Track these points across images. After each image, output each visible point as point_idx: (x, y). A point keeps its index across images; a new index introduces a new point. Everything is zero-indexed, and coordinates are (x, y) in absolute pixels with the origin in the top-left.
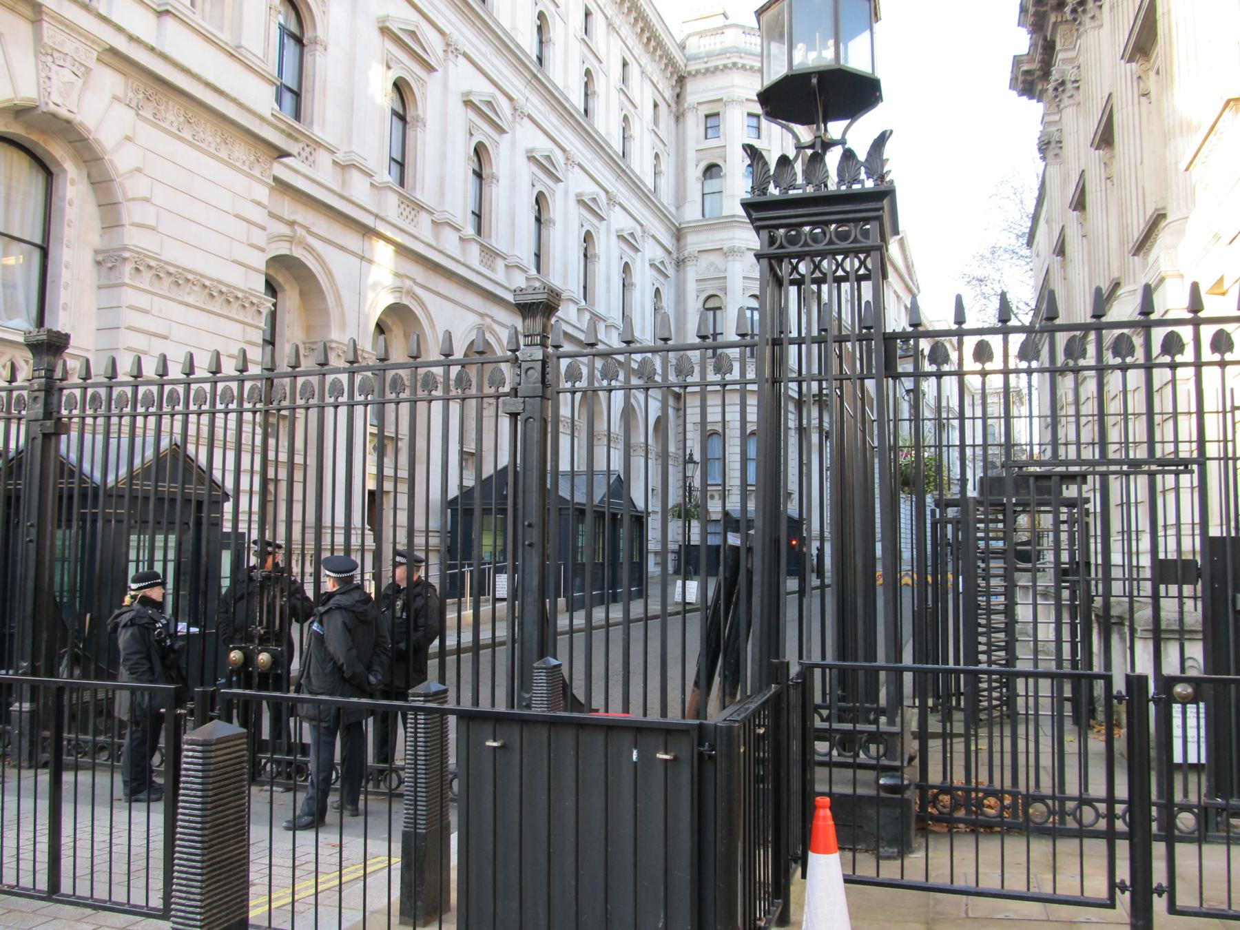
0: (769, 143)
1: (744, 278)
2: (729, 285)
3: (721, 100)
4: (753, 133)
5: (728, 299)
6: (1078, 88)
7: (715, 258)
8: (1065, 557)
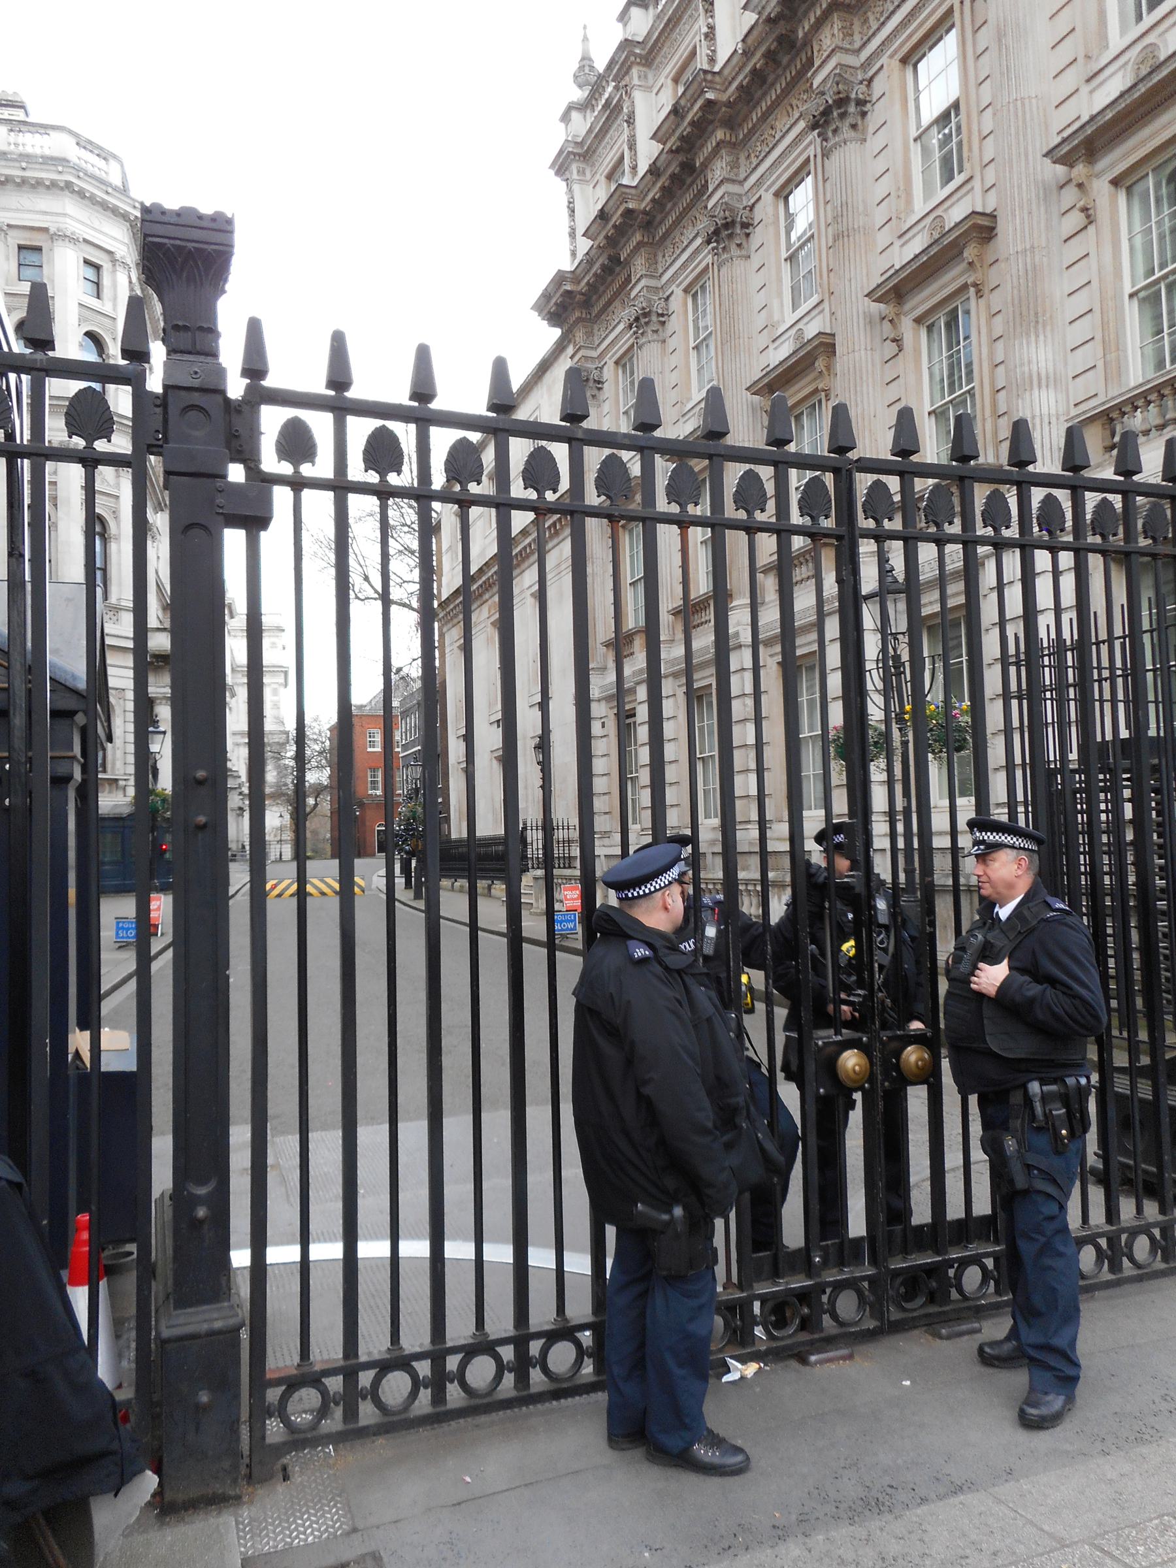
0: (115, 309)
3: (46, 230)
4: (90, 287)
5: (60, 514)
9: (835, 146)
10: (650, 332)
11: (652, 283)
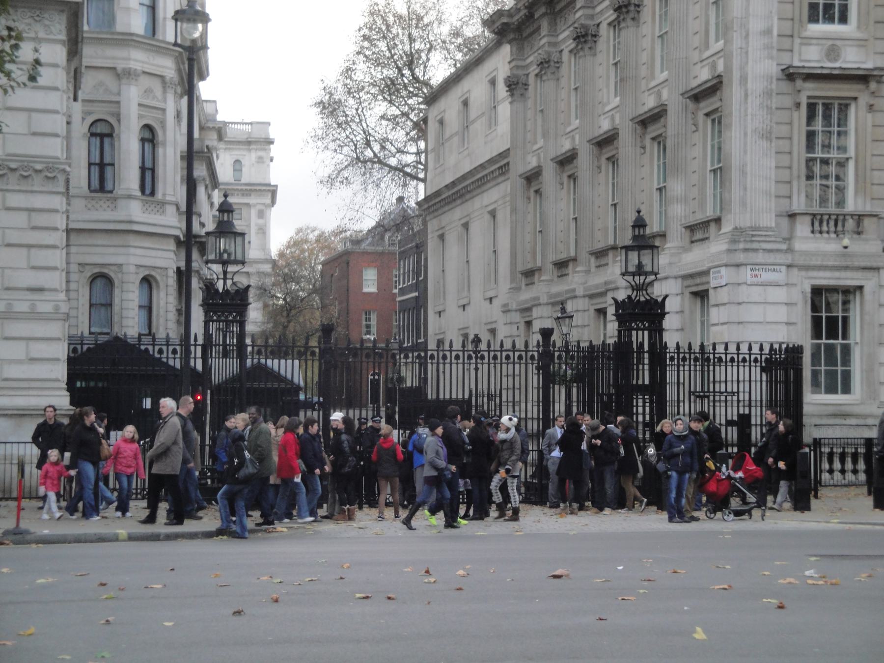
1: (140, 105)
2: (123, 111)
5: (122, 127)
6: (558, 68)
7: (108, 79)
8: (647, 418)
9: (623, 28)
10: (549, 74)
11: (553, 40)
